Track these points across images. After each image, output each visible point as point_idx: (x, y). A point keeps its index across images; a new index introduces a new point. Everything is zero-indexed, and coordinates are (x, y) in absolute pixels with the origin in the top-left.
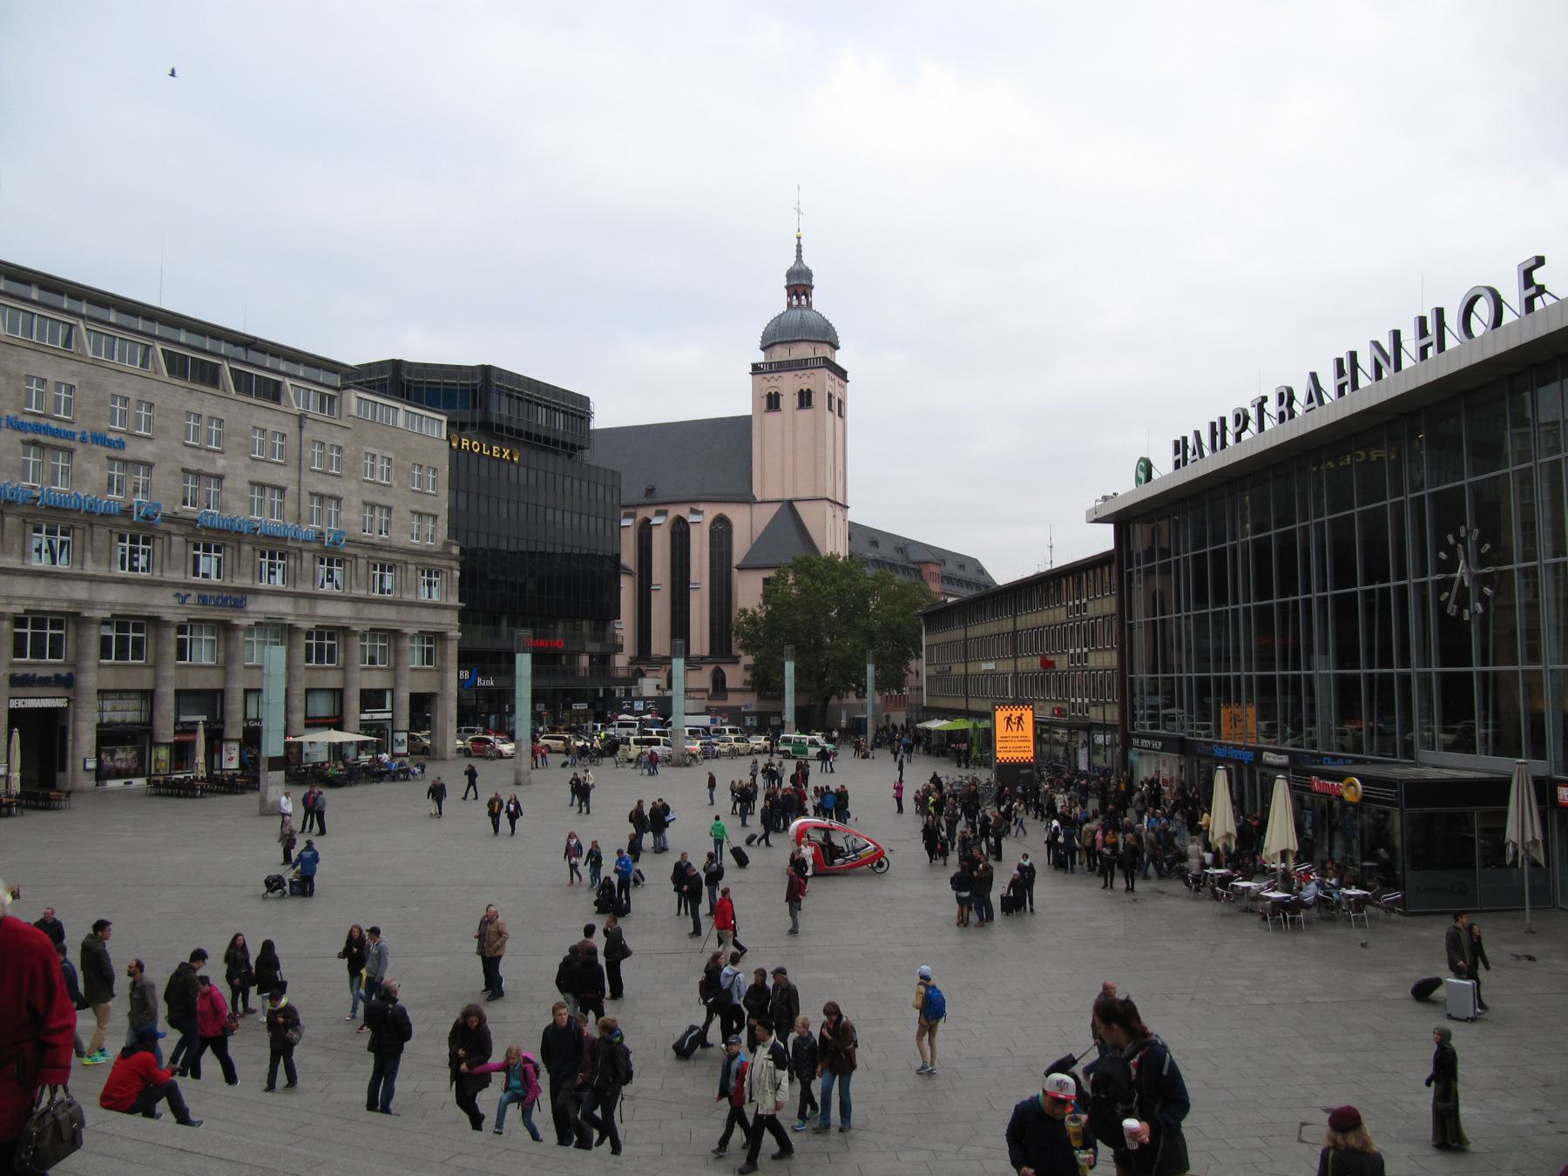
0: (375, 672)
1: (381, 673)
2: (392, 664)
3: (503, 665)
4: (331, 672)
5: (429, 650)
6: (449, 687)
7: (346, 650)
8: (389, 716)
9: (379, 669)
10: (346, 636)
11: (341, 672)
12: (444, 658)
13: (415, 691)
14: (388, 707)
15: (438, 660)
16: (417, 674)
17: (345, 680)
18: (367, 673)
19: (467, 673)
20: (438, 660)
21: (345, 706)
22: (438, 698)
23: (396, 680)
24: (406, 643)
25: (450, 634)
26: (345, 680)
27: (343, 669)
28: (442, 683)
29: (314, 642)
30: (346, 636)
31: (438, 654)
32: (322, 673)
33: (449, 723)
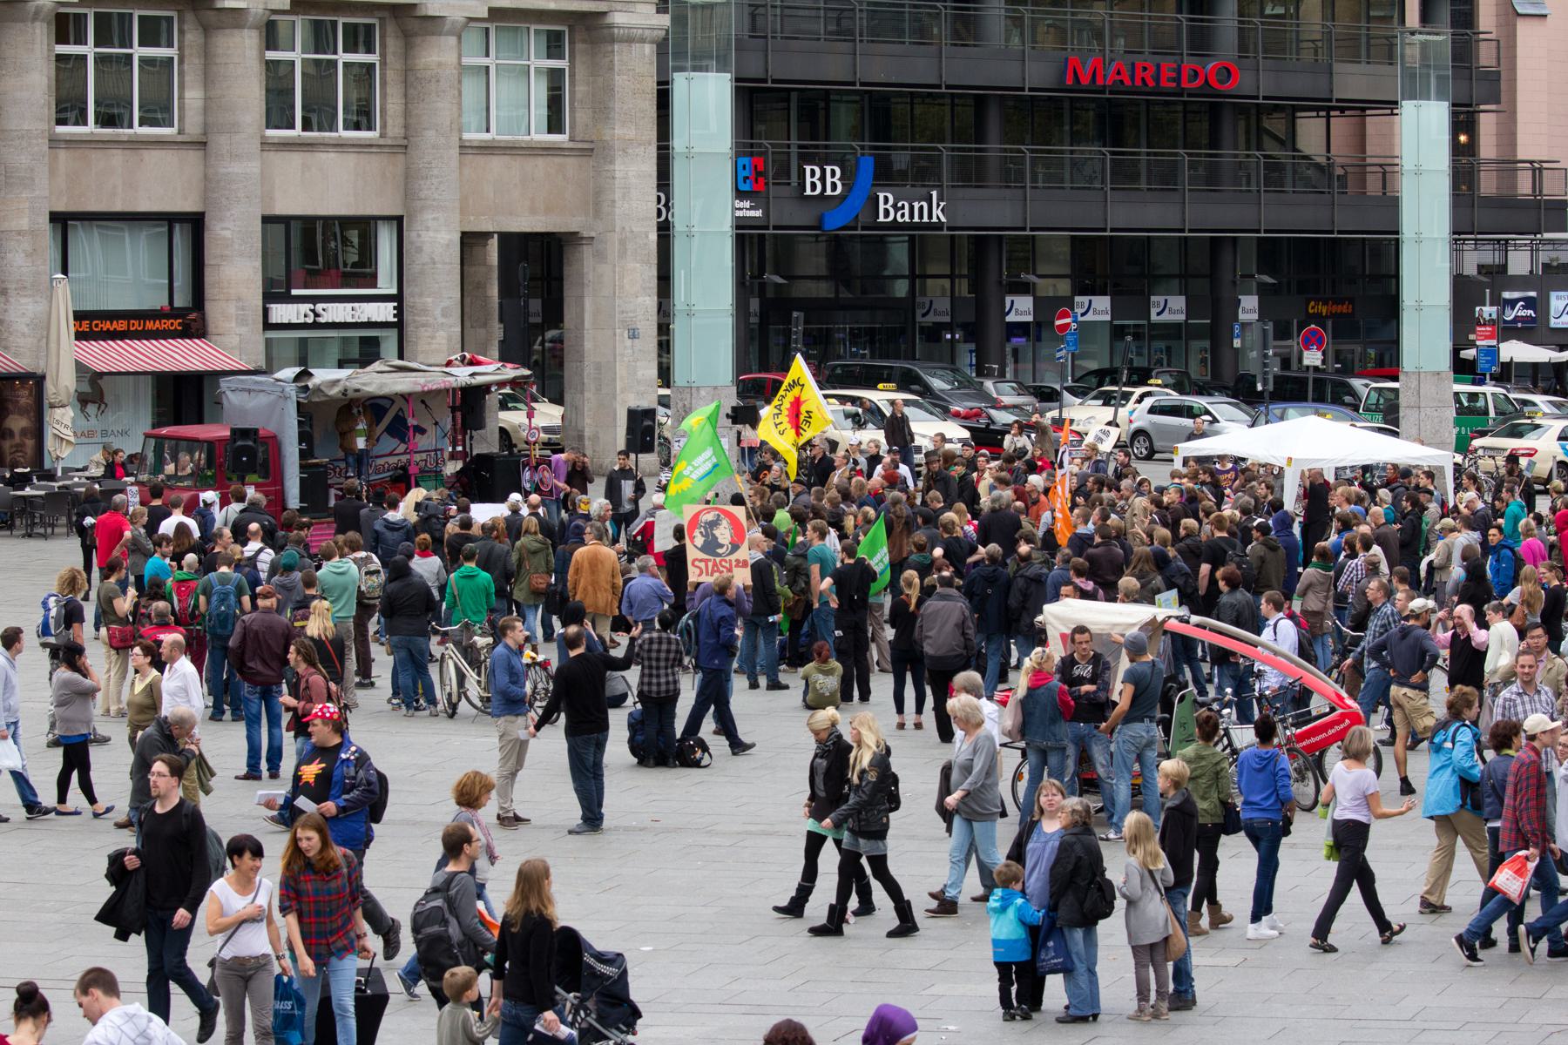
0: (328, 158)
1: (350, 160)
2: (395, 130)
3: (994, 147)
4: (152, 156)
5: (555, 78)
6: (621, 208)
7: (208, 80)
8: (385, 312)
9: (340, 146)
10: (207, 30)
11: (193, 156)
12: (602, 108)
13: (467, 230)
14: (386, 285)
15: (583, 117)
16: (496, 163)
17: (209, 183)
18: (296, 159)
19: (834, 175)
20: (583, 117)
21: (209, 277)
22: (587, 252)
23: (409, 184)
24: (439, 55)
25: (618, 19)
26: (209, 183)
27: (202, 145)
28: (597, 199)
29: (89, 50)
30: (207, 30)
31: (581, 89)
32: (117, 157)
33: (624, 345)
